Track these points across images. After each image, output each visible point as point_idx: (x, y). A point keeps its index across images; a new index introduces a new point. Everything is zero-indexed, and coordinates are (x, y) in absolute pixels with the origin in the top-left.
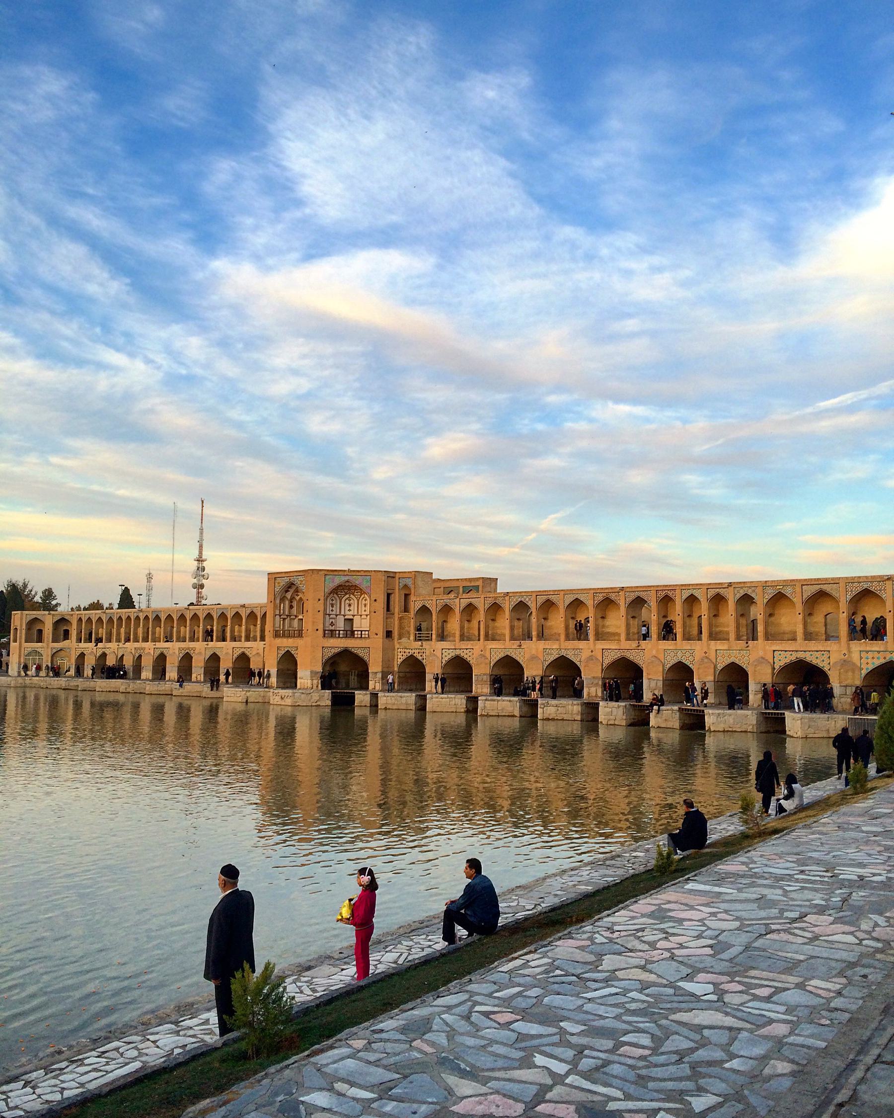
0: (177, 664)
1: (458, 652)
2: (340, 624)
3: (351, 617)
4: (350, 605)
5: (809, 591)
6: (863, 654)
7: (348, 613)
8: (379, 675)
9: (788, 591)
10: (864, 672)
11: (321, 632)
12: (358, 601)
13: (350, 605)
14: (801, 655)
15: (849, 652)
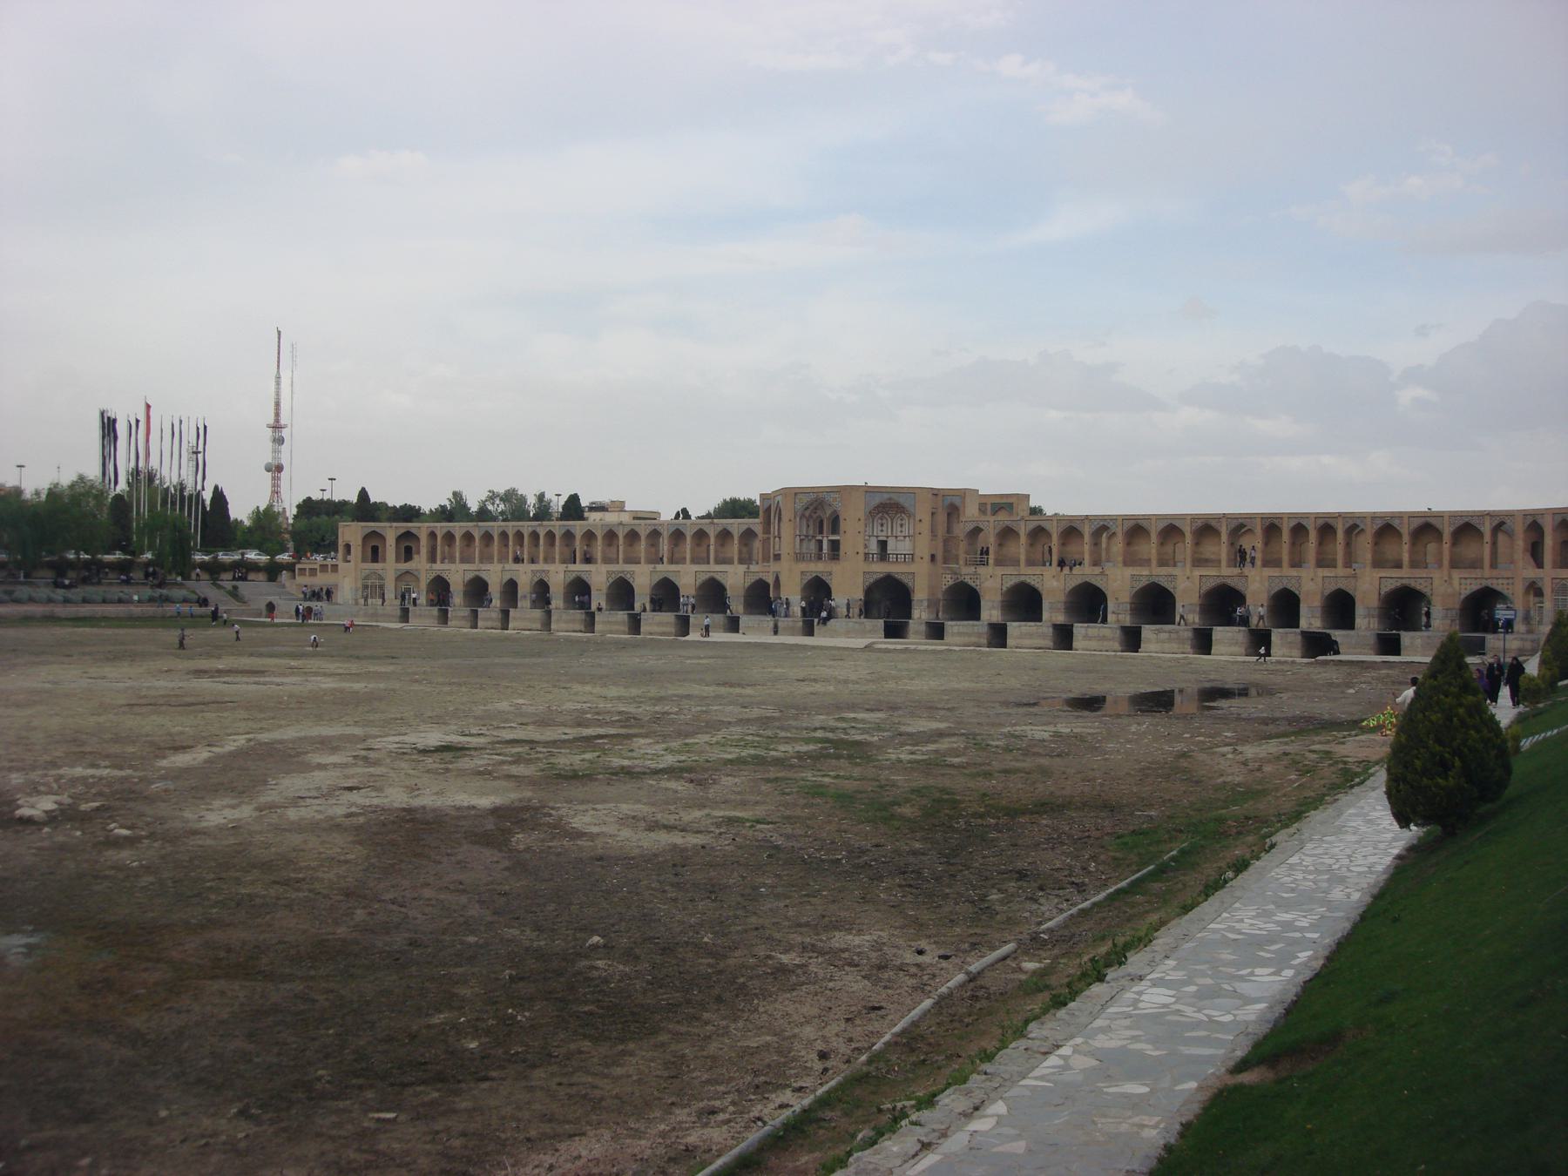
0: (605, 591)
1: (1023, 578)
2: (874, 547)
3: (885, 539)
4: (882, 525)
5: (1416, 523)
6: (1463, 581)
7: (880, 534)
8: (925, 604)
9: (1396, 523)
10: (1463, 597)
11: (861, 556)
12: (892, 520)
13: (882, 525)
14: (1405, 582)
15: (1450, 577)
